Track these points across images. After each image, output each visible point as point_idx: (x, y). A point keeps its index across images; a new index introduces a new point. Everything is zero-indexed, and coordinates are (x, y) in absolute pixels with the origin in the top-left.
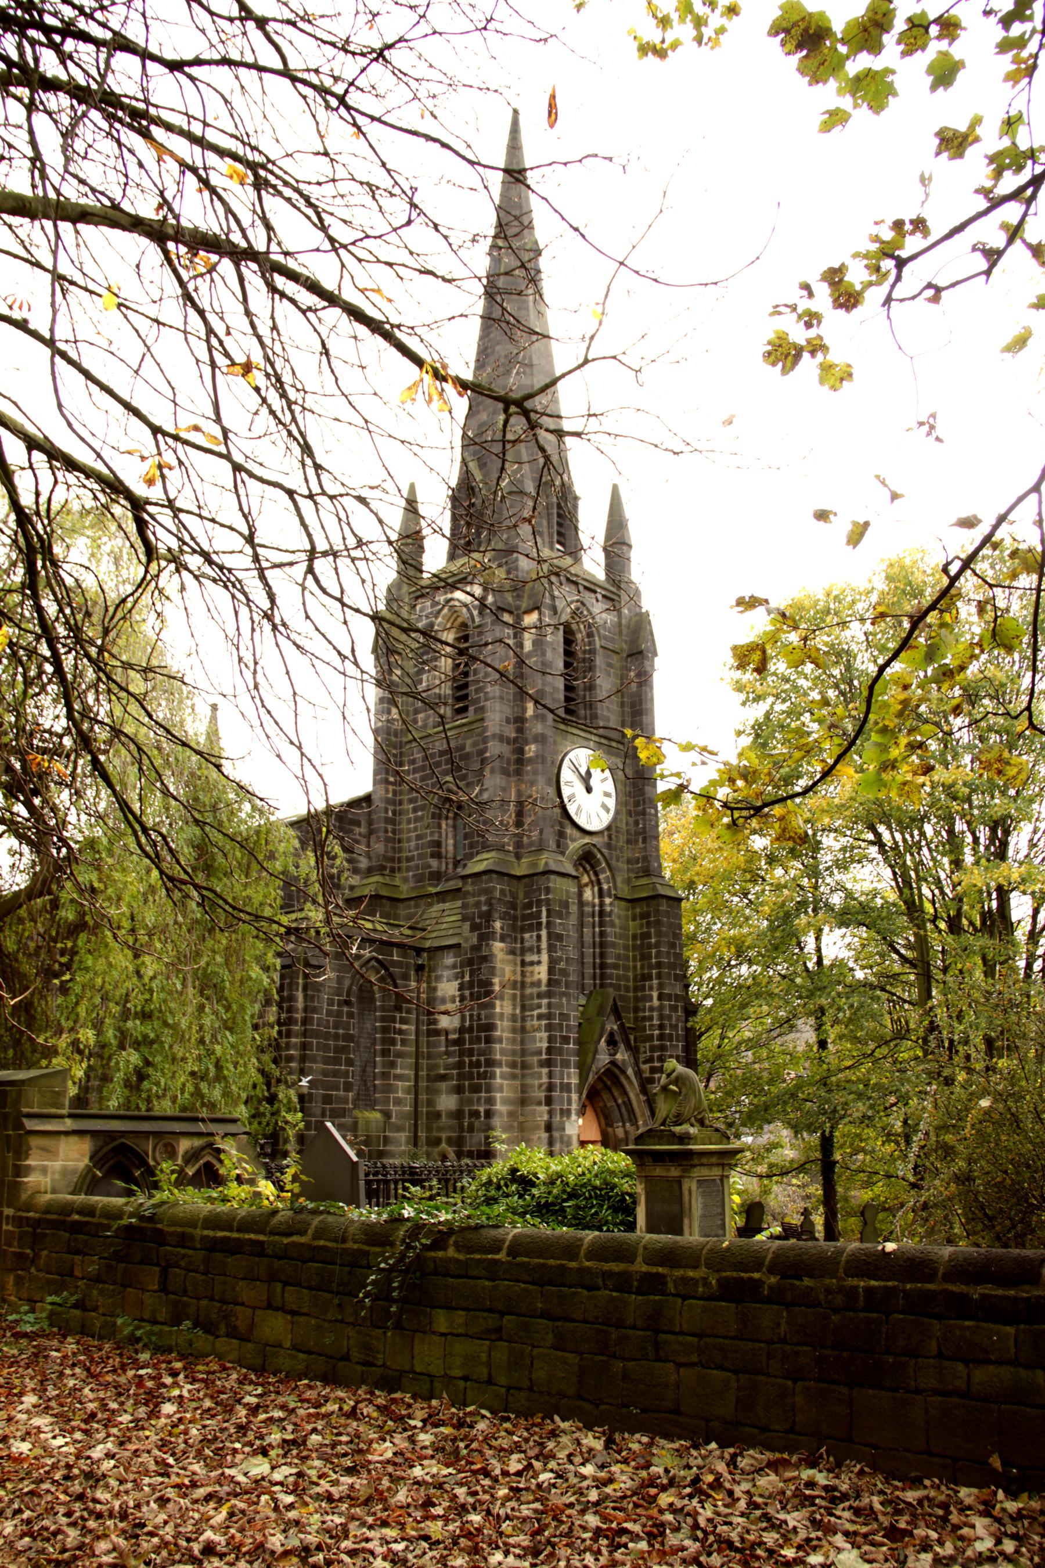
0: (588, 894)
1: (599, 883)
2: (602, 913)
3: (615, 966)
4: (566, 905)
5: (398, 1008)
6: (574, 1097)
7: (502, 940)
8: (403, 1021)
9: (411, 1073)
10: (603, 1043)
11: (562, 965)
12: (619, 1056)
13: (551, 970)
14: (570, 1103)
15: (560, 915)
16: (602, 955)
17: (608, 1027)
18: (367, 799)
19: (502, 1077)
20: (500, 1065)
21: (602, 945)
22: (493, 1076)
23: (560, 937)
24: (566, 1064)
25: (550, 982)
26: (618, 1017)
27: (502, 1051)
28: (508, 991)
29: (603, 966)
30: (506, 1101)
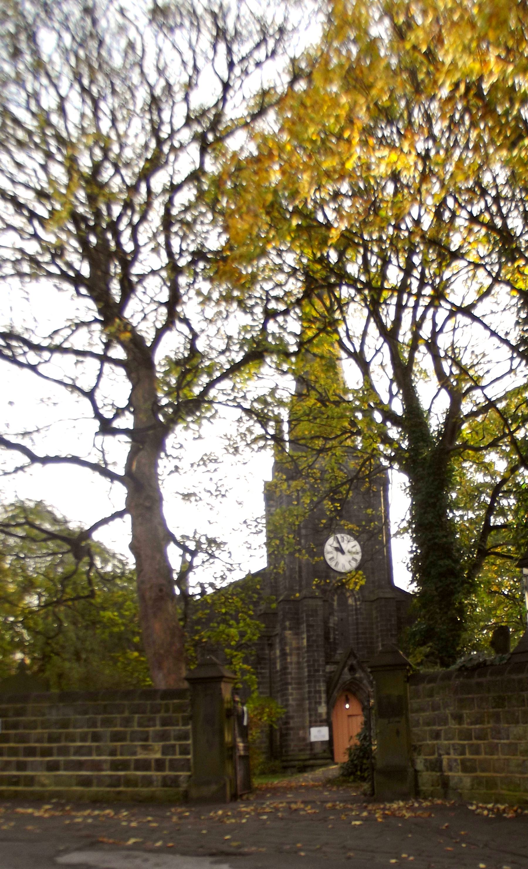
0: (350, 601)
1: (354, 595)
2: (356, 609)
3: (363, 633)
4: (316, 611)
5: (260, 663)
6: (323, 696)
7: (290, 629)
8: (262, 668)
9: (268, 691)
10: (346, 670)
11: (314, 638)
12: (357, 675)
13: (308, 641)
14: (320, 698)
15: (312, 616)
16: (357, 629)
17: (349, 663)
18: (264, 569)
19: (293, 689)
20: (291, 684)
21: (357, 624)
22: (287, 689)
23: (312, 626)
24: (319, 681)
25: (309, 646)
26: (355, 657)
27: (292, 678)
28: (295, 652)
29: (357, 634)
30: (293, 700)
